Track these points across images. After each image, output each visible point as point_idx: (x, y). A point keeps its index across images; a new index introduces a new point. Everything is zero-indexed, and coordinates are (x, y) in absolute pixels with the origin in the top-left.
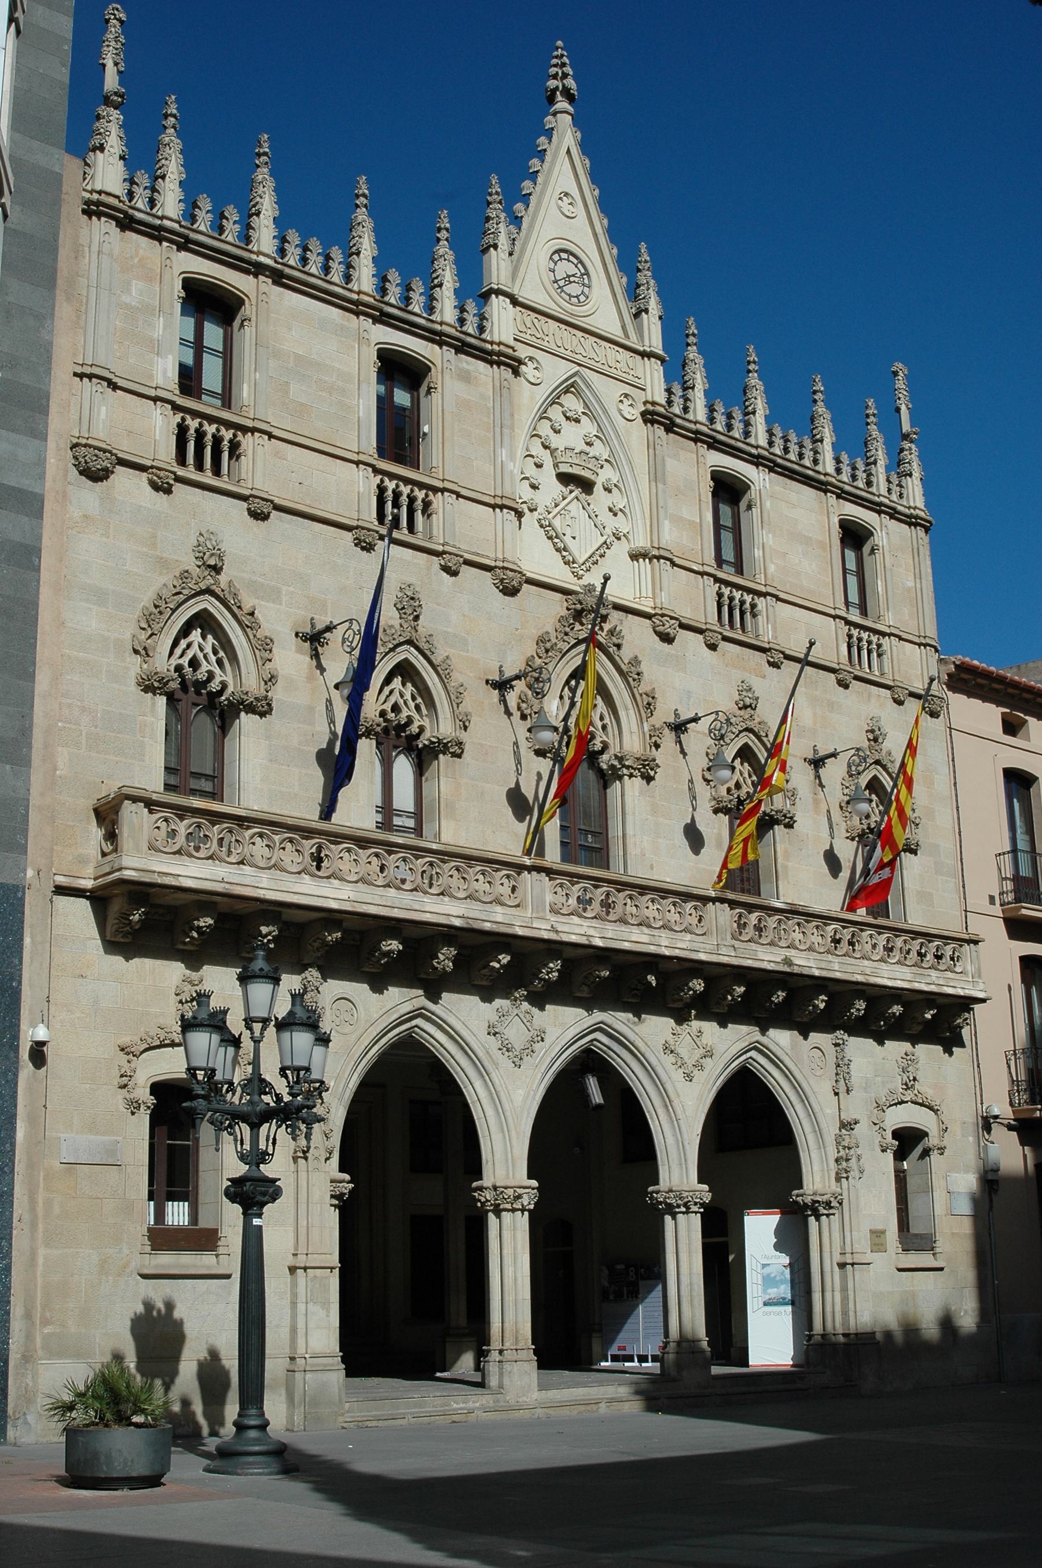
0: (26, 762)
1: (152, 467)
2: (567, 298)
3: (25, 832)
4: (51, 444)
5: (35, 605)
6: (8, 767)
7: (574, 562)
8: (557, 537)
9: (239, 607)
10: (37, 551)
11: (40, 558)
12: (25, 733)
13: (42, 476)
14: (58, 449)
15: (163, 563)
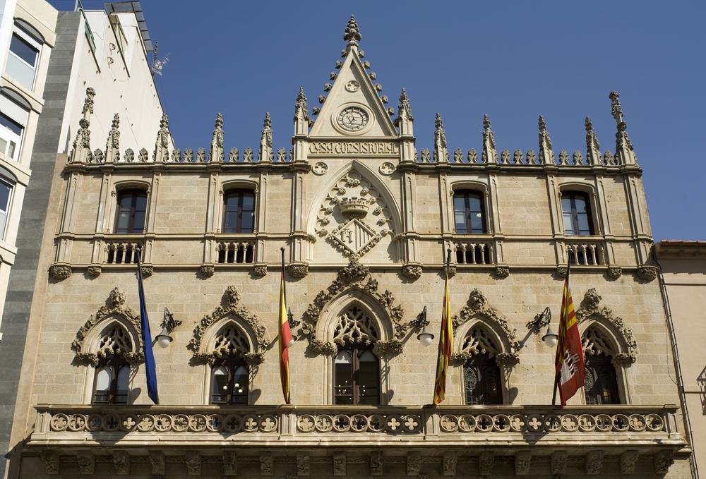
0: (14, 403)
1: (89, 267)
2: (357, 129)
3: (10, 432)
4: (40, 270)
5: (25, 337)
6: (4, 406)
7: (351, 253)
8: (340, 244)
9: (131, 317)
10: (28, 315)
11: (29, 318)
12: (14, 390)
13: (33, 284)
14: (43, 271)
15: (93, 306)
